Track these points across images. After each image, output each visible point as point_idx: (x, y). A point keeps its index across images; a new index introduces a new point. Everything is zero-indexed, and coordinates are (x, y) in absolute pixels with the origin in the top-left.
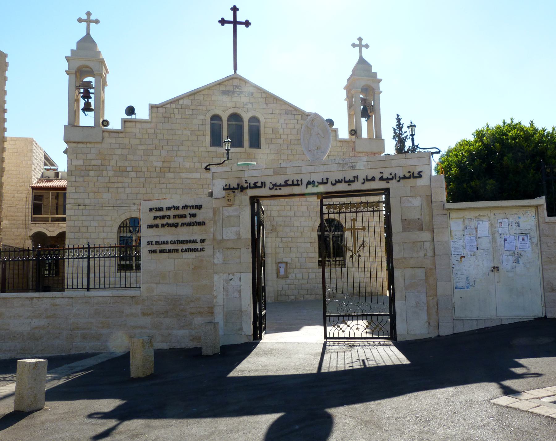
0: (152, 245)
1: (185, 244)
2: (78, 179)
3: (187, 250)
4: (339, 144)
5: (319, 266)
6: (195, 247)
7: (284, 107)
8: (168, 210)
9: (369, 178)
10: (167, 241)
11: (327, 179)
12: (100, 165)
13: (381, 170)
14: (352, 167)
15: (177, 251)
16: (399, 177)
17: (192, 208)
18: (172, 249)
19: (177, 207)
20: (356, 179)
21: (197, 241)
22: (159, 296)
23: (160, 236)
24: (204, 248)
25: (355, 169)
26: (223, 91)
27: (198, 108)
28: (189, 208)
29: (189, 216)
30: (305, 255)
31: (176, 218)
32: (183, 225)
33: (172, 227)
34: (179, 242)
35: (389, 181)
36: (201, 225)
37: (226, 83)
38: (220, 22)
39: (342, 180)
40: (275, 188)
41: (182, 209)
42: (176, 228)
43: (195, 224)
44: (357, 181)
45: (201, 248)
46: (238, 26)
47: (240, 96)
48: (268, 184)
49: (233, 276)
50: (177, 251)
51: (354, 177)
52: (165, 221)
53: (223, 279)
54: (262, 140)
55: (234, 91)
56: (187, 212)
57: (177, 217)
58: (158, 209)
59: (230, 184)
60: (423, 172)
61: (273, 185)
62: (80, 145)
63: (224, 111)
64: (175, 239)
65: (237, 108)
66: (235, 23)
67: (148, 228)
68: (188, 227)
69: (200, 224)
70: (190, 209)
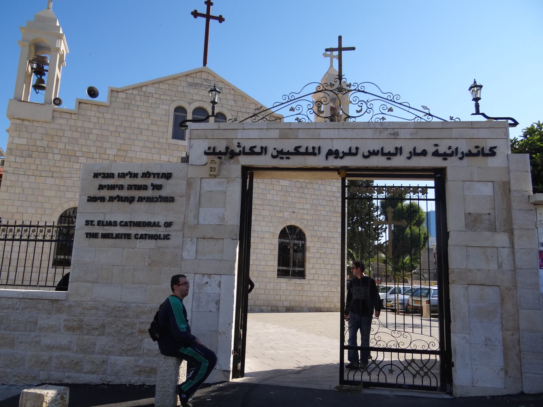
0: (93, 226)
1: (142, 228)
2: (18, 160)
3: (144, 236)
5: (277, 275)
6: (156, 234)
8: (121, 177)
9: (419, 151)
10: (115, 222)
11: (357, 149)
12: (46, 146)
13: (436, 142)
14: (394, 134)
15: (128, 236)
16: (462, 153)
17: (156, 176)
18: (122, 234)
19: (134, 173)
20: (399, 151)
21: (160, 224)
22: (96, 301)
23: (105, 214)
24: (169, 235)
25: (398, 137)
26: (191, 82)
27: (162, 97)
28: (152, 176)
29: (152, 187)
30: (263, 263)
31: (131, 189)
32: (141, 199)
33: (124, 201)
34: (132, 224)
35: (447, 158)
36: (167, 201)
37: (194, 75)
38: (192, 13)
39: (378, 151)
40: (280, 156)
41: (142, 177)
42: (130, 203)
43: (160, 200)
44: (401, 154)
45: (164, 235)
46: (212, 21)
48: (270, 151)
49: (210, 278)
50: (128, 236)
51: (396, 149)
52: (115, 193)
53: (194, 283)
55: (202, 84)
56: (148, 182)
57: (133, 188)
58: (106, 175)
59: (215, 147)
60: (497, 148)
61: (278, 151)
62: (26, 123)
63: (190, 104)
64: (126, 218)
65: (204, 101)
66: (208, 17)
67: (88, 201)
68: (148, 204)
69: (166, 200)
70: (154, 177)
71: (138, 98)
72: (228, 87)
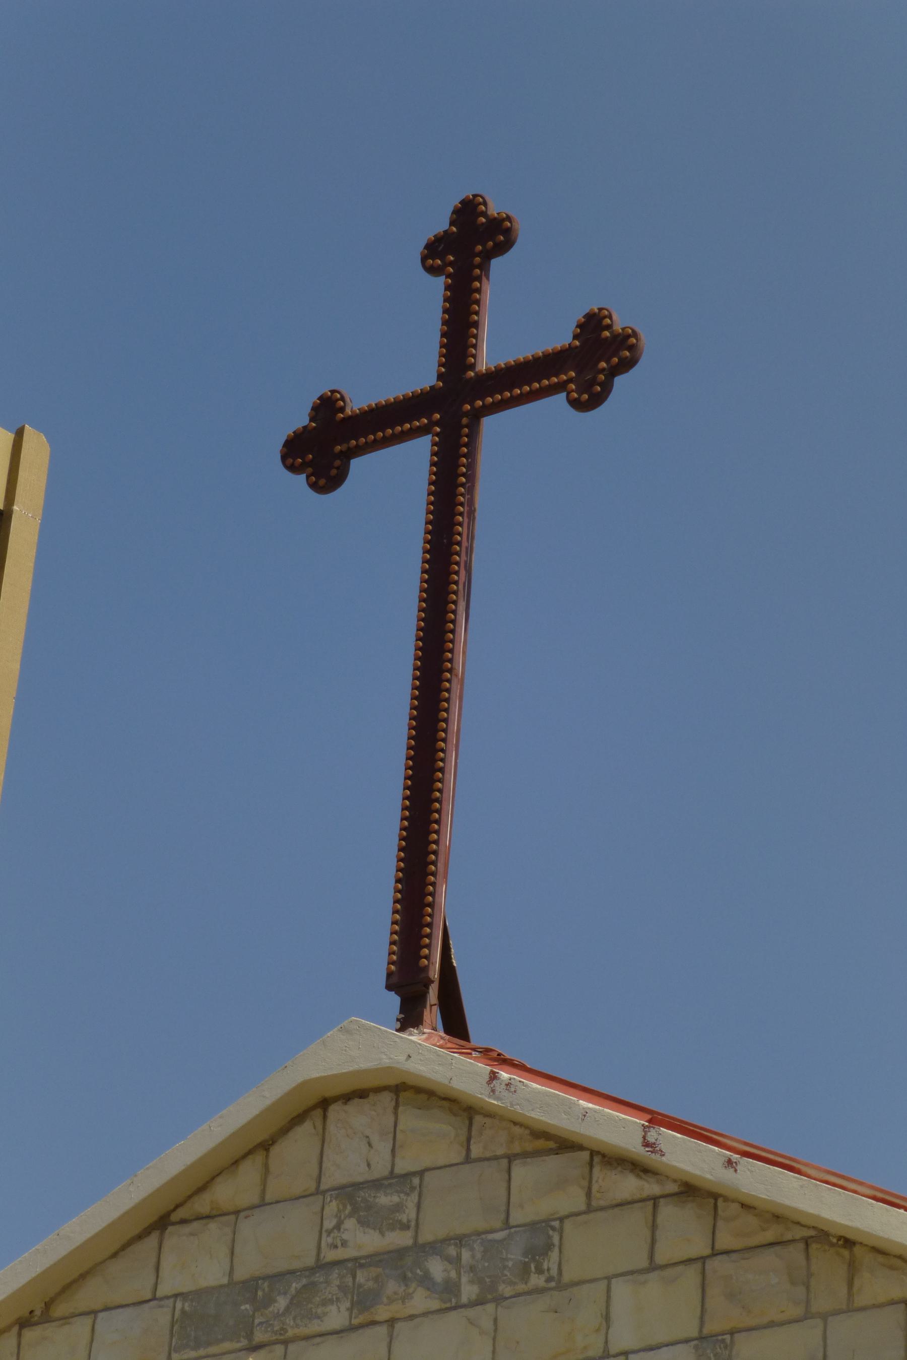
47: (382, 1313)
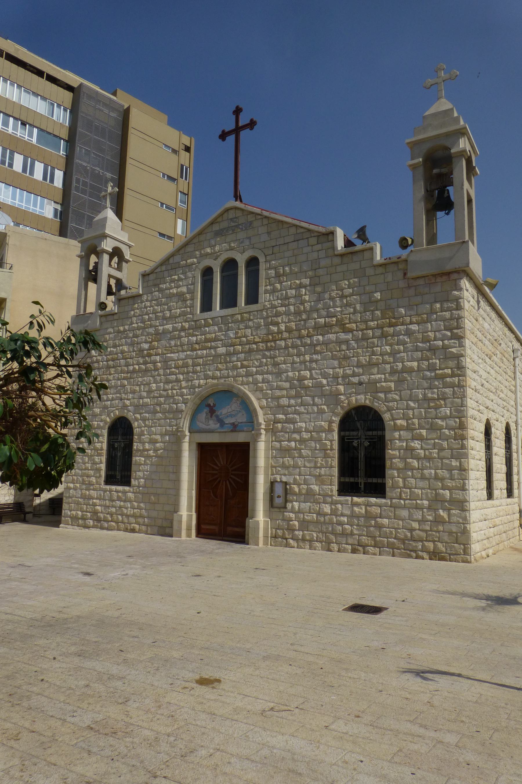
4: (380, 270)
7: (292, 230)
37: (219, 220)
54: (262, 289)
66: (237, 130)
71: (166, 274)
72: (260, 217)
